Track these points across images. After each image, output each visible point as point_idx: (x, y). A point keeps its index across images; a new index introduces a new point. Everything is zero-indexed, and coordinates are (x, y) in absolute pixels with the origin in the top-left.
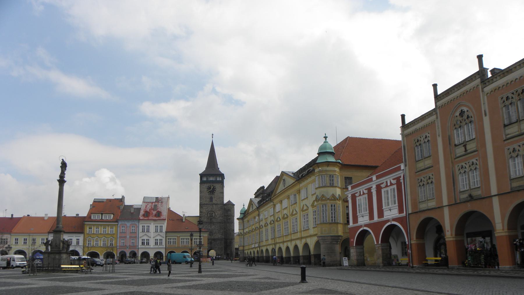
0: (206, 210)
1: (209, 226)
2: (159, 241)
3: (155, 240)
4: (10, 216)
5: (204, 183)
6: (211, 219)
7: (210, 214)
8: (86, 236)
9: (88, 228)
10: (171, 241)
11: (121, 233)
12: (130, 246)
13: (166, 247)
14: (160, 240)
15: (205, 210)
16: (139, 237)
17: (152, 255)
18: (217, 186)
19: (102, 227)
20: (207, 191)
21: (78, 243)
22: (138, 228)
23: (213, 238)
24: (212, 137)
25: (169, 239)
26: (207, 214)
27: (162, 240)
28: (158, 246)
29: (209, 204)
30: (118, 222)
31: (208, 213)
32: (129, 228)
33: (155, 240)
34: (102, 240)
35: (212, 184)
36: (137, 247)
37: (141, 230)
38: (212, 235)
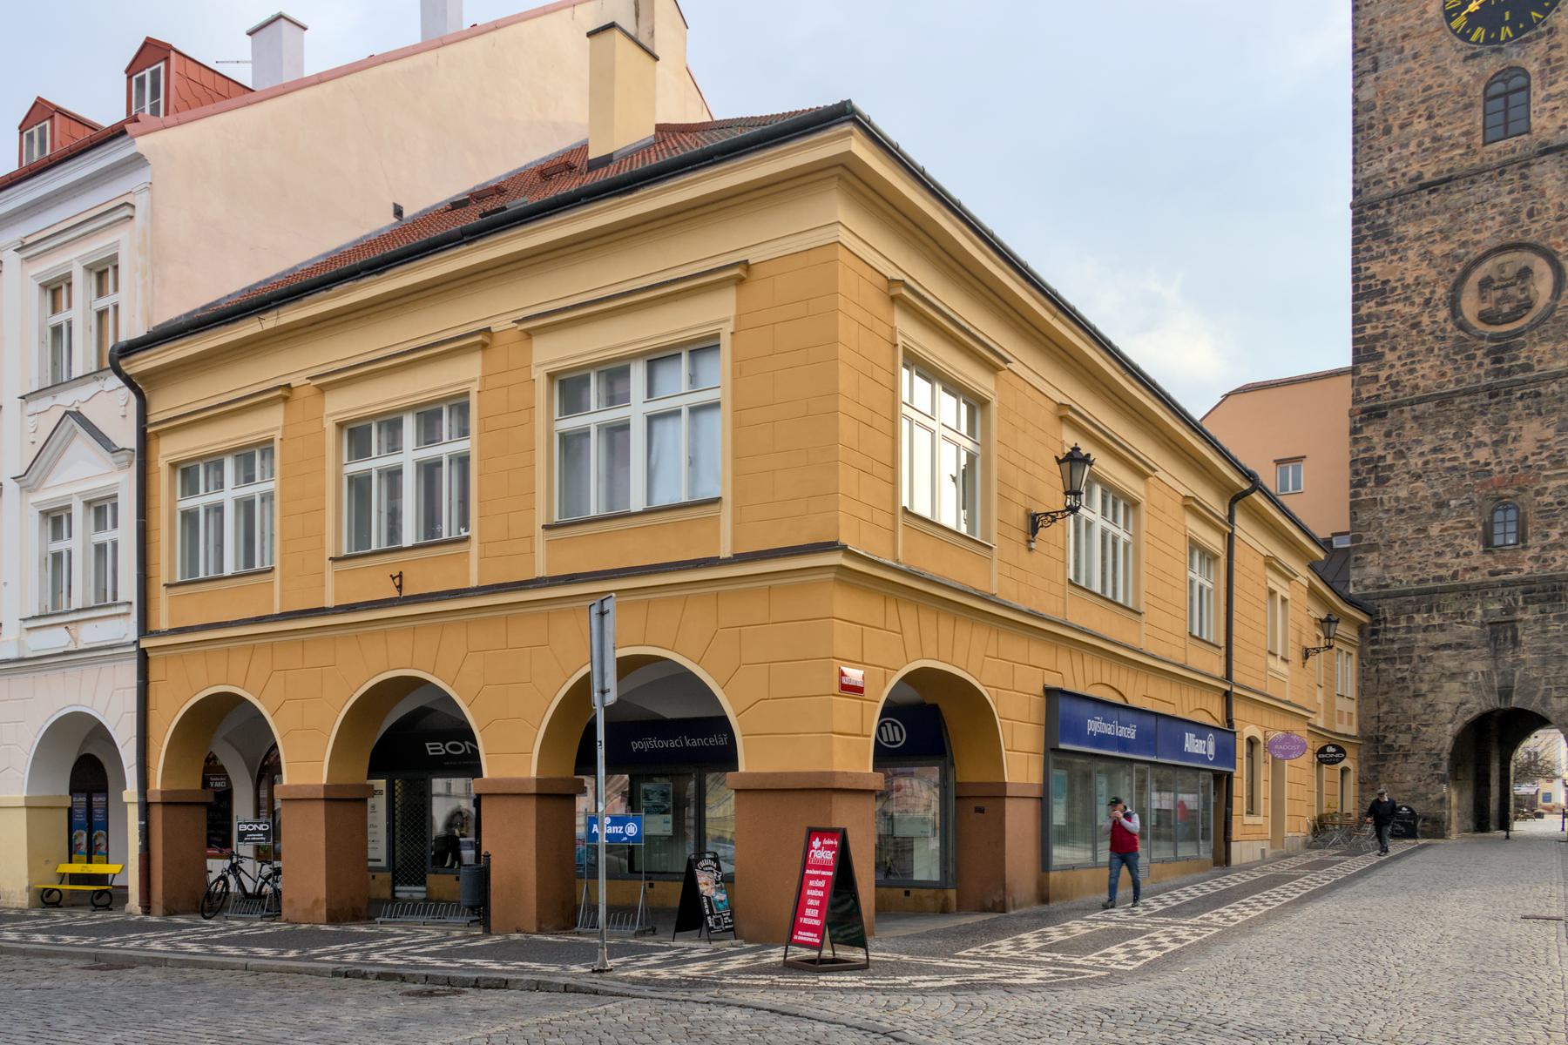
0: (1438, 250)
1: (1479, 430)
6: (1497, 354)
7: (1485, 284)
15: (1426, 256)
23: (1527, 567)
26: (1454, 303)
29: (1472, 175)
31: (1466, 273)
38: (1522, 537)
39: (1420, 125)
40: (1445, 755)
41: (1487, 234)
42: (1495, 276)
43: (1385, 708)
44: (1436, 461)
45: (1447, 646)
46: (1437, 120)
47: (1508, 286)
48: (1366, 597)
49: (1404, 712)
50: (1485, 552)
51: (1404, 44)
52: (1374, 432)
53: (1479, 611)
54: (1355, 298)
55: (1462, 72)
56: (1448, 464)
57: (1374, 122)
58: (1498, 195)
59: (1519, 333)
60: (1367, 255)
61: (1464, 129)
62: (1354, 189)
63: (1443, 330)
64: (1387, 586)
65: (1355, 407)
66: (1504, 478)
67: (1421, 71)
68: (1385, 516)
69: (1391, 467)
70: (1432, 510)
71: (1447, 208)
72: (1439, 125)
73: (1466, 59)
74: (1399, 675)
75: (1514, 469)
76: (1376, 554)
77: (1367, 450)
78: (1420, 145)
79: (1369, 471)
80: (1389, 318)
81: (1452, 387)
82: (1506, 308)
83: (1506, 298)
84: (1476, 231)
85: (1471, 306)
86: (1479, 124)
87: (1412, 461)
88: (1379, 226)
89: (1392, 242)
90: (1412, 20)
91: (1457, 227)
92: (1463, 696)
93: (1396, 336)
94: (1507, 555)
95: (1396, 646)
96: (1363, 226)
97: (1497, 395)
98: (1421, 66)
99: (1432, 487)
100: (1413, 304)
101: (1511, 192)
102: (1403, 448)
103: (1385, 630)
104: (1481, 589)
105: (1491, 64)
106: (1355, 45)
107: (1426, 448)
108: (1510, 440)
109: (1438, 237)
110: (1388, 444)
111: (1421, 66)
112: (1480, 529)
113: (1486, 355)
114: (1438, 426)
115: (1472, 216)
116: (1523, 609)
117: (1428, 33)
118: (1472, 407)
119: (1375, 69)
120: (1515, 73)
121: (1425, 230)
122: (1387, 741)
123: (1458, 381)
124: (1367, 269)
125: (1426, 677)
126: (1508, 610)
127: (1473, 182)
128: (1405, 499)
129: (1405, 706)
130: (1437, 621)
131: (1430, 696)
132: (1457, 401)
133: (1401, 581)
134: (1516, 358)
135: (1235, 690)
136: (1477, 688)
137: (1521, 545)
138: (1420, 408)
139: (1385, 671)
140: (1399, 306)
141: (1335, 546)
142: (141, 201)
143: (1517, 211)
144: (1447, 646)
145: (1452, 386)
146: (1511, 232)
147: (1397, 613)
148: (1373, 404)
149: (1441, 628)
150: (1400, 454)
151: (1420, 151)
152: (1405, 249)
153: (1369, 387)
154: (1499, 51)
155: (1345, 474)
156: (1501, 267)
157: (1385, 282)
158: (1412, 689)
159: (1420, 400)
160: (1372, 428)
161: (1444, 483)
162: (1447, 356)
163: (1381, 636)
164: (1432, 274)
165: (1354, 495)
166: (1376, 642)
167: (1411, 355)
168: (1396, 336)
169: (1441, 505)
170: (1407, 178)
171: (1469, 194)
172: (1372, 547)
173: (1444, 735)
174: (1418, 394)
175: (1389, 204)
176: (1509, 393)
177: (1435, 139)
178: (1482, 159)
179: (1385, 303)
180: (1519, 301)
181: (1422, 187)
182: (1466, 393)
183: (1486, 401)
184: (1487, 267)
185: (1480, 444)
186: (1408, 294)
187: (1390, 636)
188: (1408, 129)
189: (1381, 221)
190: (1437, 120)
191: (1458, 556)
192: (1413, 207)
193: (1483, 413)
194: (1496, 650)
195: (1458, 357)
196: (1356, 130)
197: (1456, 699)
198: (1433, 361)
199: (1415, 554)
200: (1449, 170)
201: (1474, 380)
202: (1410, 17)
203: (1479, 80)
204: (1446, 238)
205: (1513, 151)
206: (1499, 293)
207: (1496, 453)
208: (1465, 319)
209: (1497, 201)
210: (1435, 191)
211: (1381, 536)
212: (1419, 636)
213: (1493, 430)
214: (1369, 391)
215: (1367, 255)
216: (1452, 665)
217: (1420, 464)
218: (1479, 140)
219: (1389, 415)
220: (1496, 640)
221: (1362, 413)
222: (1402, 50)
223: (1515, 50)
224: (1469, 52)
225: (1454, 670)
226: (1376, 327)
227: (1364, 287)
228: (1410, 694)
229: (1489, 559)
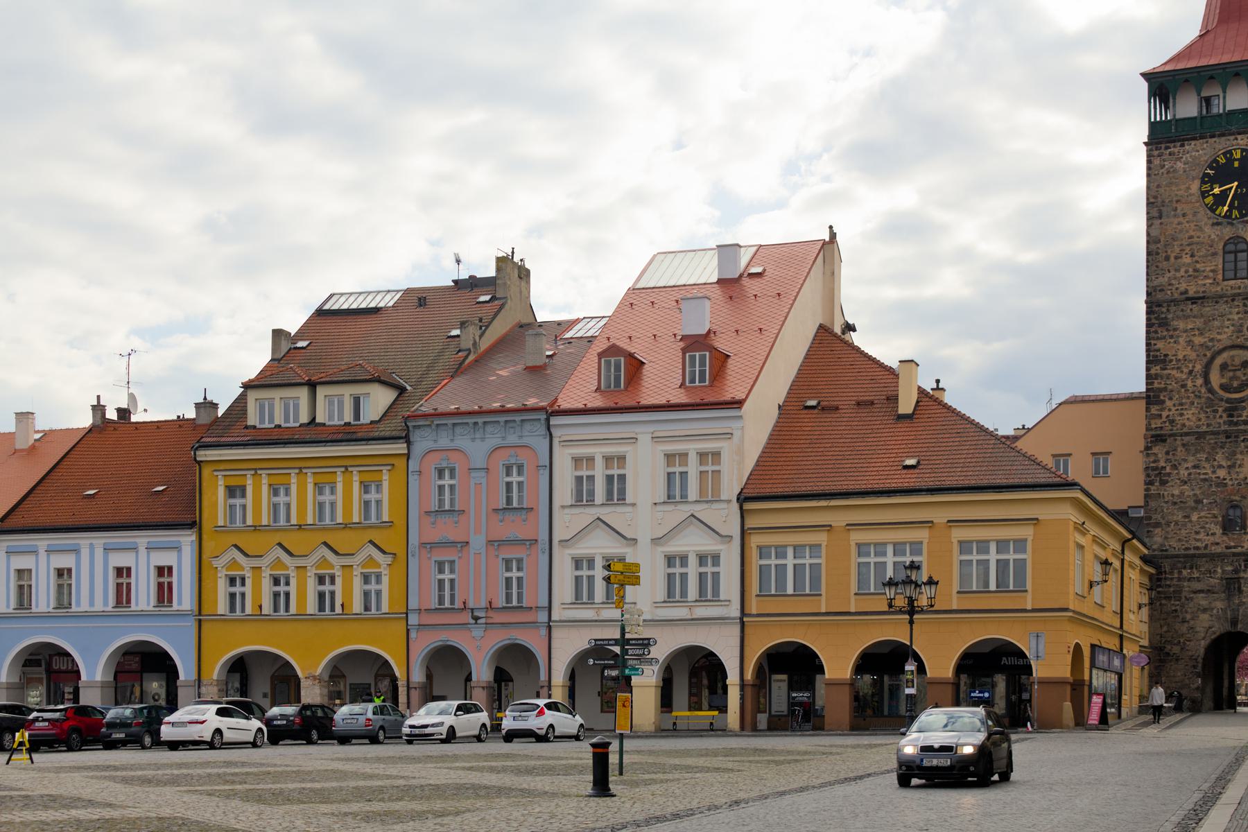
0: (1198, 340)
1: (1220, 458)
2: (693, 570)
3: (670, 560)
7: (1224, 367)
8: (208, 545)
9: (221, 492)
10: (781, 569)
11: (428, 513)
12: (490, 606)
13: (743, 613)
14: (702, 559)
15: (1190, 342)
16: (557, 537)
19: (310, 479)
20: (1204, 194)
21: (164, 593)
25: (763, 551)
26: (1206, 376)
28: (690, 608)
29: (1217, 298)
30: (409, 443)
31: (1213, 358)
32: (479, 477)
33: (670, 560)
34: (357, 572)
37: (564, 491)
39: (1187, 259)
40: (1200, 660)
41: (1223, 337)
42: (1229, 362)
43: (1165, 629)
44: (1196, 473)
45: (1201, 591)
46: (1196, 258)
47: (1236, 370)
48: (1154, 556)
49: (1176, 632)
50: (1223, 534)
51: (1178, 206)
52: (1159, 450)
53: (1219, 570)
54: (1148, 362)
55: (1211, 233)
56: (1202, 477)
57: (1160, 251)
58: (1231, 313)
59: (1242, 400)
60: (1156, 336)
61: (1212, 268)
62: (1147, 292)
63: (1200, 392)
64: (1166, 550)
65: (1148, 433)
66: (1234, 489)
67: (1187, 225)
68: (1165, 505)
69: (1169, 474)
70: (1193, 504)
71: (1202, 316)
72: (1197, 262)
73: (1213, 224)
74: (1174, 608)
75: (1239, 484)
76: (1160, 529)
77: (1154, 462)
78: (1186, 272)
79: (1156, 475)
80: (1168, 378)
81: (1204, 428)
82: (1235, 384)
83: (1236, 378)
84: (1218, 333)
85: (1216, 379)
86: (1221, 266)
87: (1182, 472)
88: (1162, 319)
89: (1169, 330)
90: (1182, 192)
91: (1207, 329)
92: (1210, 623)
93: (1172, 391)
94: (1235, 536)
95: (1172, 589)
96: (1152, 316)
97: (1230, 437)
98: (1187, 222)
99: (1193, 490)
100: (1182, 372)
101: (1238, 313)
102: (1176, 463)
103: (1165, 579)
104: (1221, 557)
105: (1228, 232)
106: (1148, 199)
107: (1190, 465)
108: (1237, 466)
109: (1197, 333)
110: (1168, 459)
111: (1187, 222)
112: (1220, 519)
113: (1224, 411)
114: (1197, 451)
115: (1216, 323)
116: (1244, 571)
117: (1191, 202)
118: (1216, 443)
119: (1160, 217)
120: (1241, 240)
121: (1190, 327)
122: (1166, 650)
123: (1208, 425)
124: (1155, 344)
125: (1189, 610)
126: (1236, 571)
127: (1217, 302)
128: (1178, 496)
129: (1177, 628)
130: (1196, 575)
131: (1192, 622)
132: (1208, 437)
133: (1175, 548)
134: (1241, 416)
135: (1124, 634)
136: (1219, 618)
137: (1243, 531)
138: (1186, 439)
139: (1165, 605)
140: (1174, 372)
141: (1130, 515)
142: (737, 434)
143: (1241, 325)
144: (1201, 591)
145: (1205, 427)
146: (1238, 337)
147: (1173, 568)
148: (1159, 432)
149: (1198, 580)
150: (1175, 467)
151: (1186, 275)
152: (1178, 337)
153: (1157, 421)
154: (1232, 224)
155: (1142, 478)
156: (1232, 358)
157: (1166, 355)
158: (1181, 617)
159: (1187, 434)
160: (1157, 447)
161: (1200, 488)
162: (1202, 408)
163: (1163, 583)
164: (1193, 355)
165: (1147, 490)
166: (1160, 586)
167: (1181, 404)
168: (1172, 391)
169: (1198, 502)
170: (1179, 291)
171: (1214, 309)
172: (1157, 525)
173: (1199, 647)
174: (1185, 430)
175: (1169, 306)
176: (1237, 437)
177: (1196, 270)
178: (1222, 289)
179: (1166, 369)
180: (1243, 381)
181: (1188, 299)
182: (1213, 433)
183: (1224, 440)
184: (1225, 355)
185: (1220, 466)
186: (1179, 365)
187: (1168, 583)
188: (1180, 260)
189: (1163, 316)
190: (1196, 258)
191: (1208, 535)
192: (1182, 310)
193: (1222, 447)
194: (1229, 595)
195: (1208, 410)
196: (1149, 253)
197: (1207, 625)
198: (1194, 410)
199: (1183, 531)
200: (1204, 292)
201: (1217, 426)
202: (1180, 190)
203: (1220, 239)
204: (1201, 334)
205: (1239, 288)
206: (1231, 374)
207: (1229, 473)
208: (1212, 386)
209: (1230, 317)
210: (1195, 303)
211: (1163, 518)
212: (1185, 584)
213: (1228, 459)
214: (1156, 424)
215: (1156, 336)
216: (1204, 603)
217: (1186, 474)
218: (1220, 277)
219: (1168, 441)
220: (1229, 589)
221: (1152, 437)
222: (1176, 209)
223: (1240, 226)
224: (1215, 221)
225: (1206, 607)
226: (1161, 383)
227: (1153, 356)
228: (1180, 620)
229: (1225, 538)
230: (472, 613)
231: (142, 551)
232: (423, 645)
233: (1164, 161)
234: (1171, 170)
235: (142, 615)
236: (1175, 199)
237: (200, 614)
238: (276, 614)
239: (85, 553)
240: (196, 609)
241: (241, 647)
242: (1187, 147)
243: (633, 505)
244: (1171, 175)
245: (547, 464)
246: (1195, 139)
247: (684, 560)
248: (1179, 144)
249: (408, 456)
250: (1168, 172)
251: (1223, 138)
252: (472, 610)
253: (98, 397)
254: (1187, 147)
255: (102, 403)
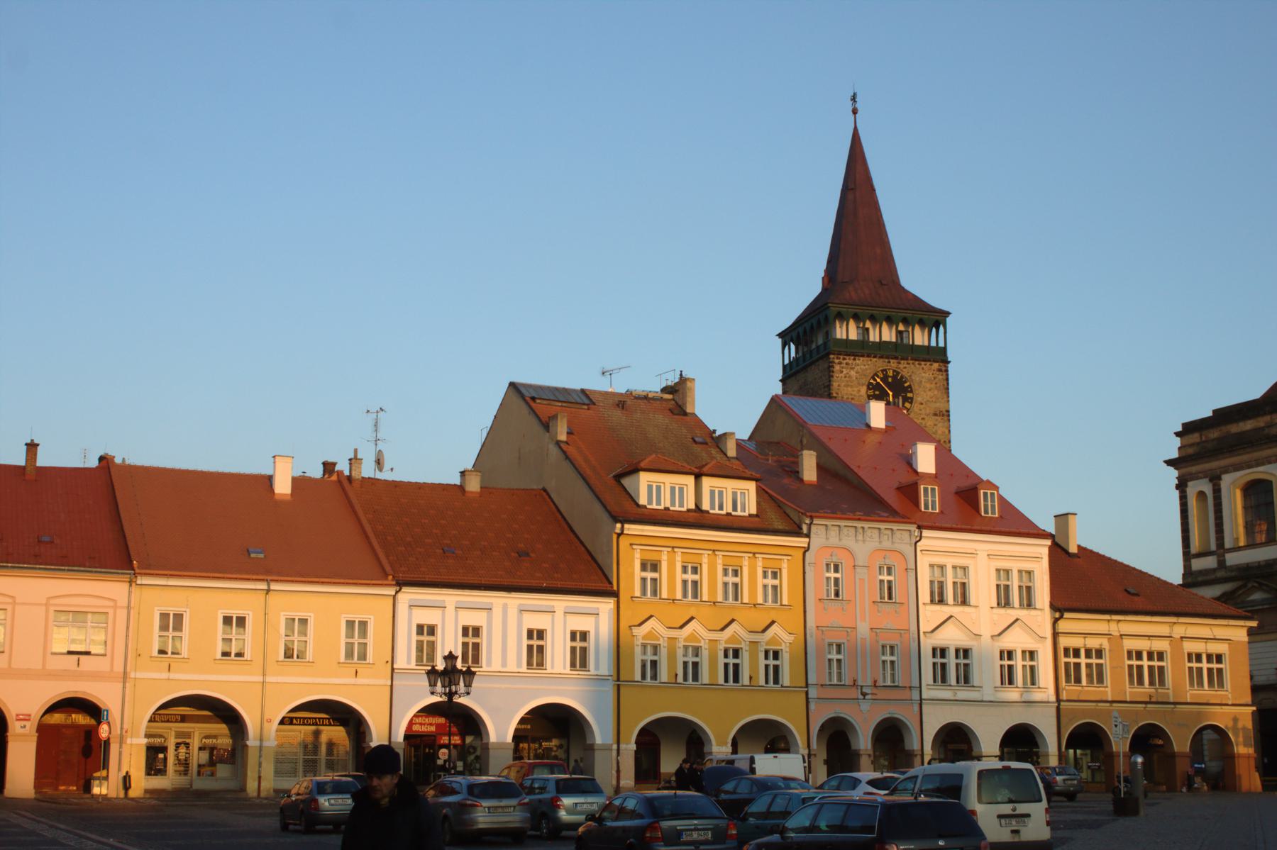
4: (19, 459)
5: (855, 355)
10: (1077, 666)
17: (989, 740)
18: (919, 375)
22: (912, 574)
24: (855, 112)
27: (1032, 654)
35: (893, 364)
36: (915, 695)
230: (861, 689)
231: (559, 614)
232: (820, 716)
233: (842, 368)
234: (848, 375)
235: (559, 677)
236: (850, 397)
237: (618, 680)
238: (726, 684)
239: (497, 612)
240: (613, 672)
241: (658, 713)
242: (857, 361)
243: (976, 607)
244: (847, 379)
245: (914, 567)
246: (863, 356)
247: (1010, 654)
248: (853, 357)
249: (807, 549)
250: (845, 377)
251: (882, 360)
252: (862, 686)
253: (356, 451)
254: (857, 361)
255: (359, 457)
